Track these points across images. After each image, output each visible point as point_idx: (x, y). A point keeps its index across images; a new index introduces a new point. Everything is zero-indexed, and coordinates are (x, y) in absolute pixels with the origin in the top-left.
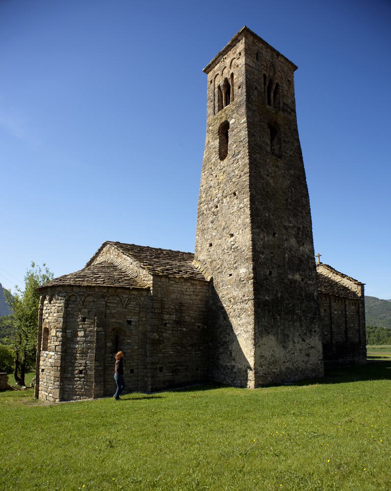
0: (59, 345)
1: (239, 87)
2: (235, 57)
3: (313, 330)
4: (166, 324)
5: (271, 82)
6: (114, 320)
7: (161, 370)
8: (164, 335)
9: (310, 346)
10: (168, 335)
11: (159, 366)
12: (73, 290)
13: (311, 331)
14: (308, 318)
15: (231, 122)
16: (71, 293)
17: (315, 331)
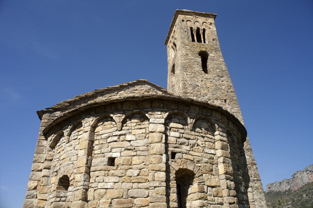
0: (234, 203)
1: (213, 40)
2: (207, 22)
12: (228, 125)
15: (211, 55)
16: (227, 127)
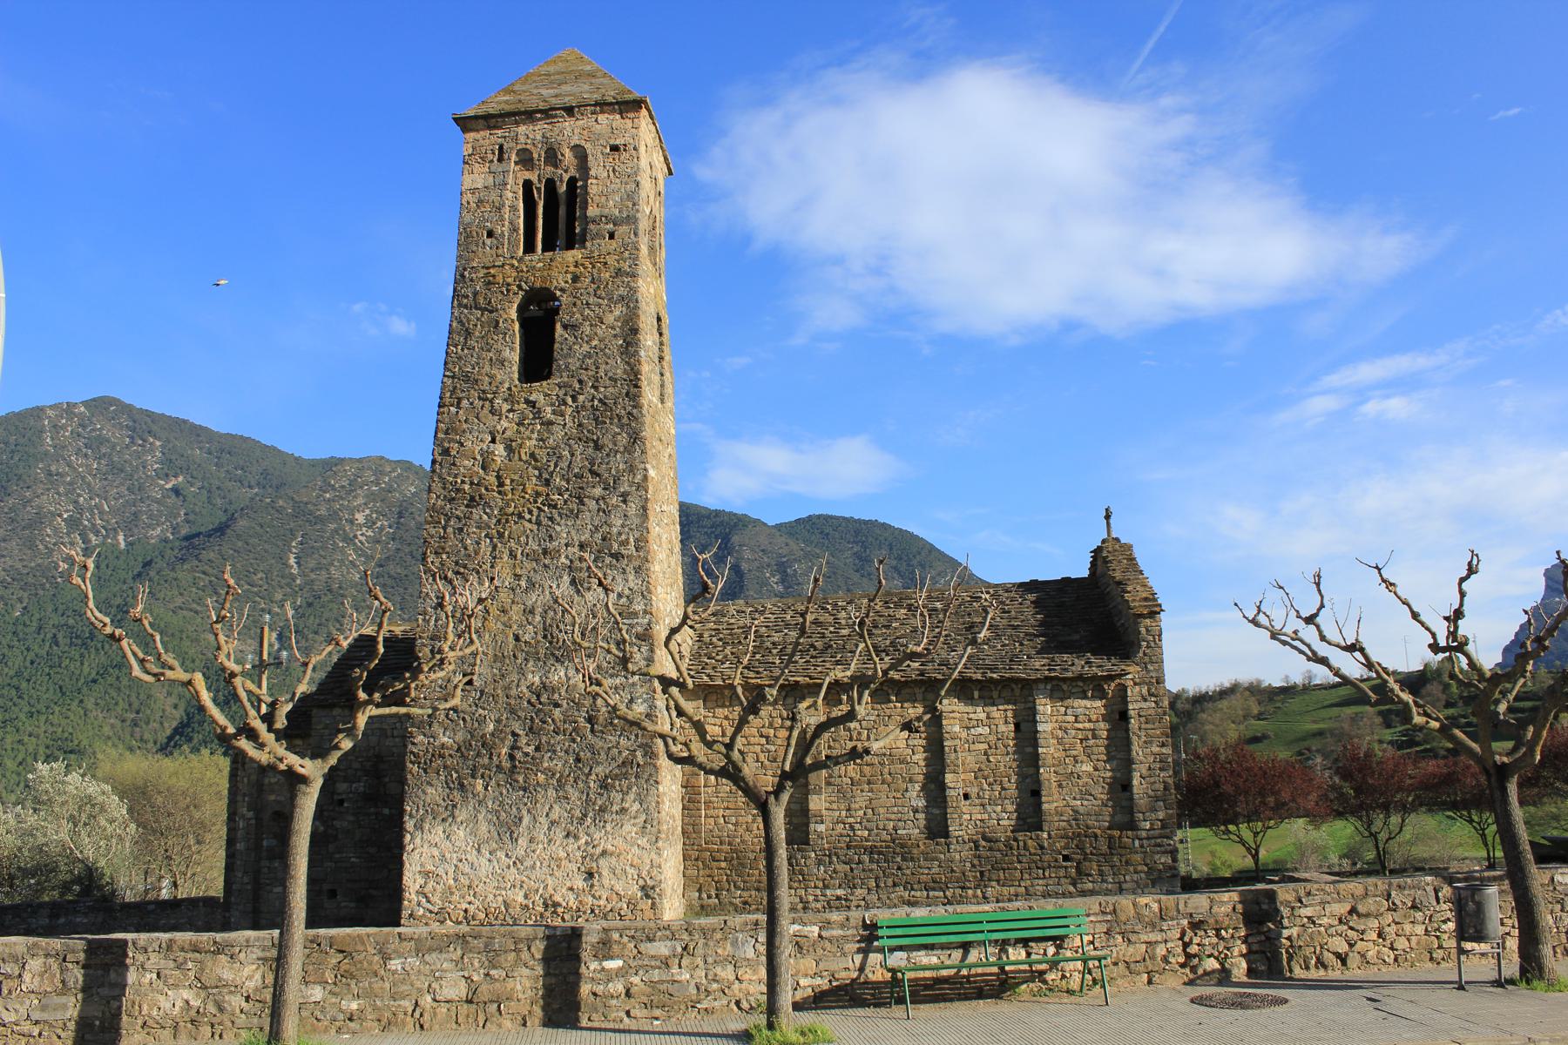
3: (615, 808)
4: (341, 802)
5: (551, 185)
6: (272, 797)
7: (333, 894)
8: (337, 824)
9: (598, 850)
10: (345, 824)
11: (326, 887)
13: (602, 810)
14: (593, 777)
17: (623, 811)
